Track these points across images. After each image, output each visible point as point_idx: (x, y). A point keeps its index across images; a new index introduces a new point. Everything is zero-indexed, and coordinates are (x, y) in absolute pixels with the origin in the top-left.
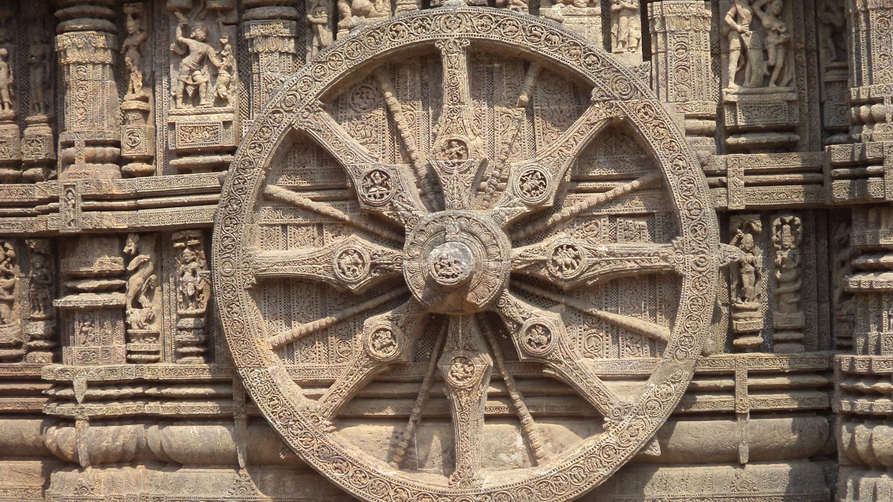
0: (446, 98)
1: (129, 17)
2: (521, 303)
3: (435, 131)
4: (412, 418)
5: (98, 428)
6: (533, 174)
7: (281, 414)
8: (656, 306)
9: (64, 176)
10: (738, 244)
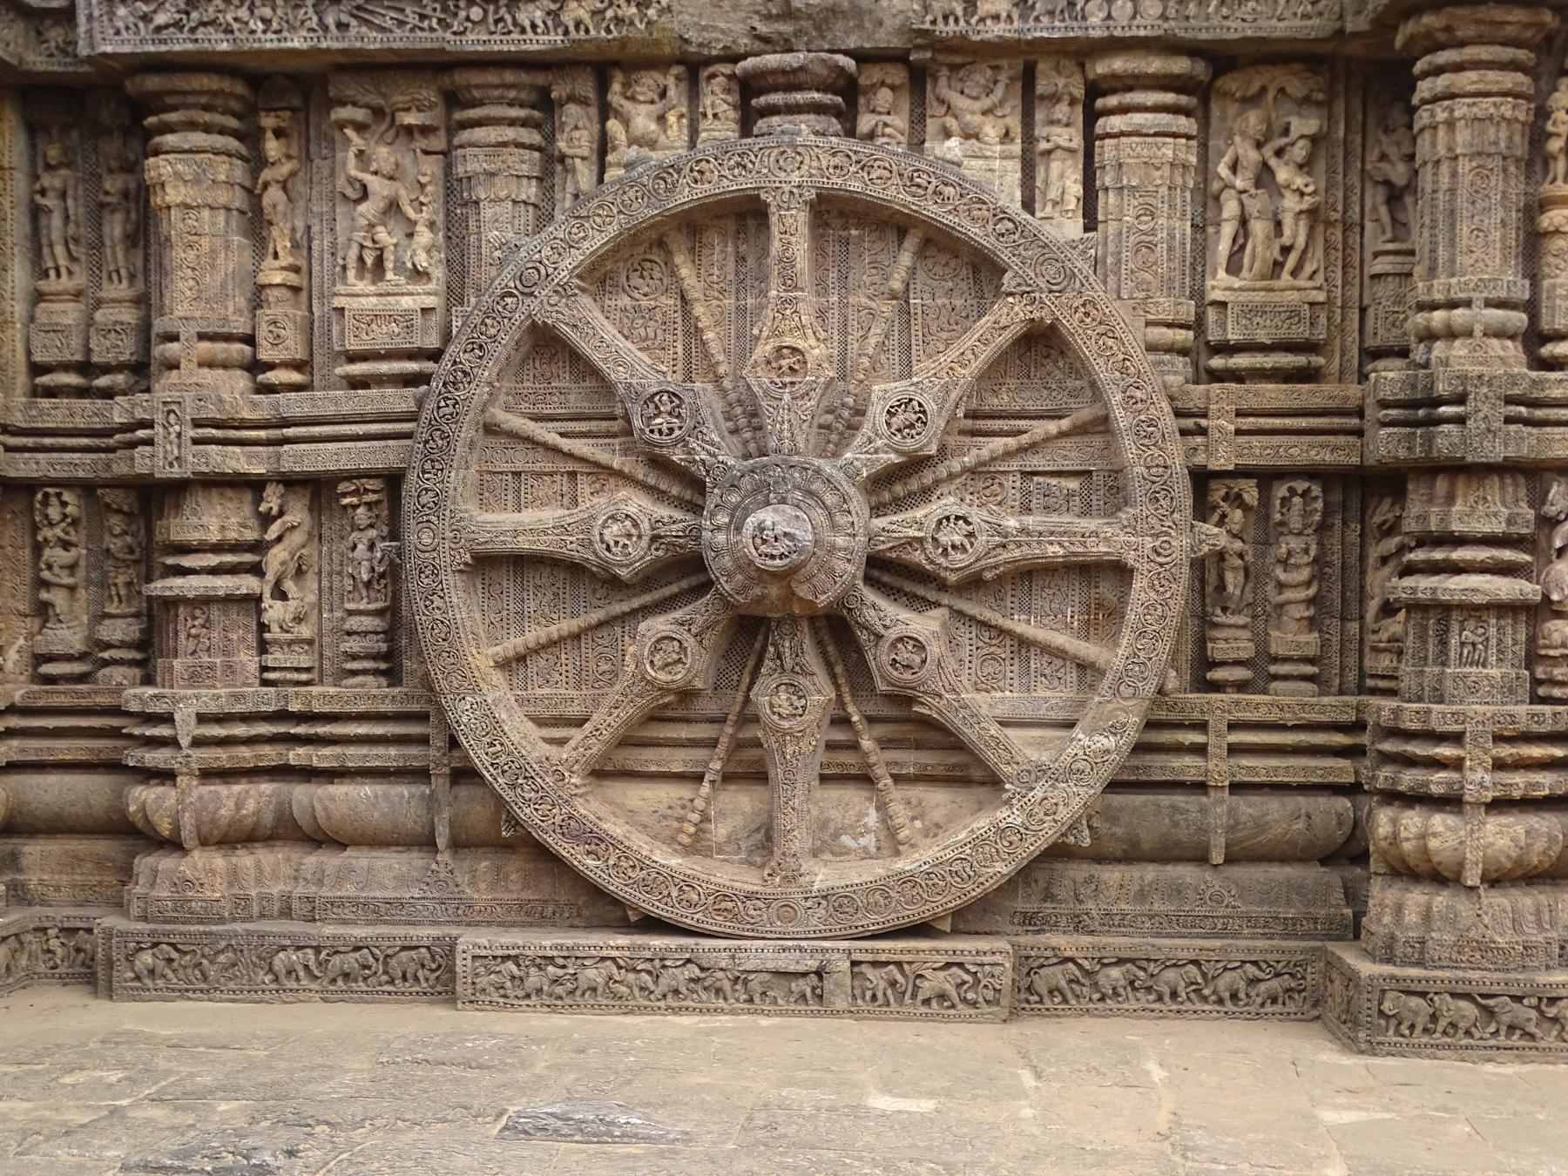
0: (775, 281)
1: (269, 134)
2: (882, 603)
3: (756, 332)
5: (213, 788)
8: (1088, 614)
9: (165, 387)
10: (1221, 523)
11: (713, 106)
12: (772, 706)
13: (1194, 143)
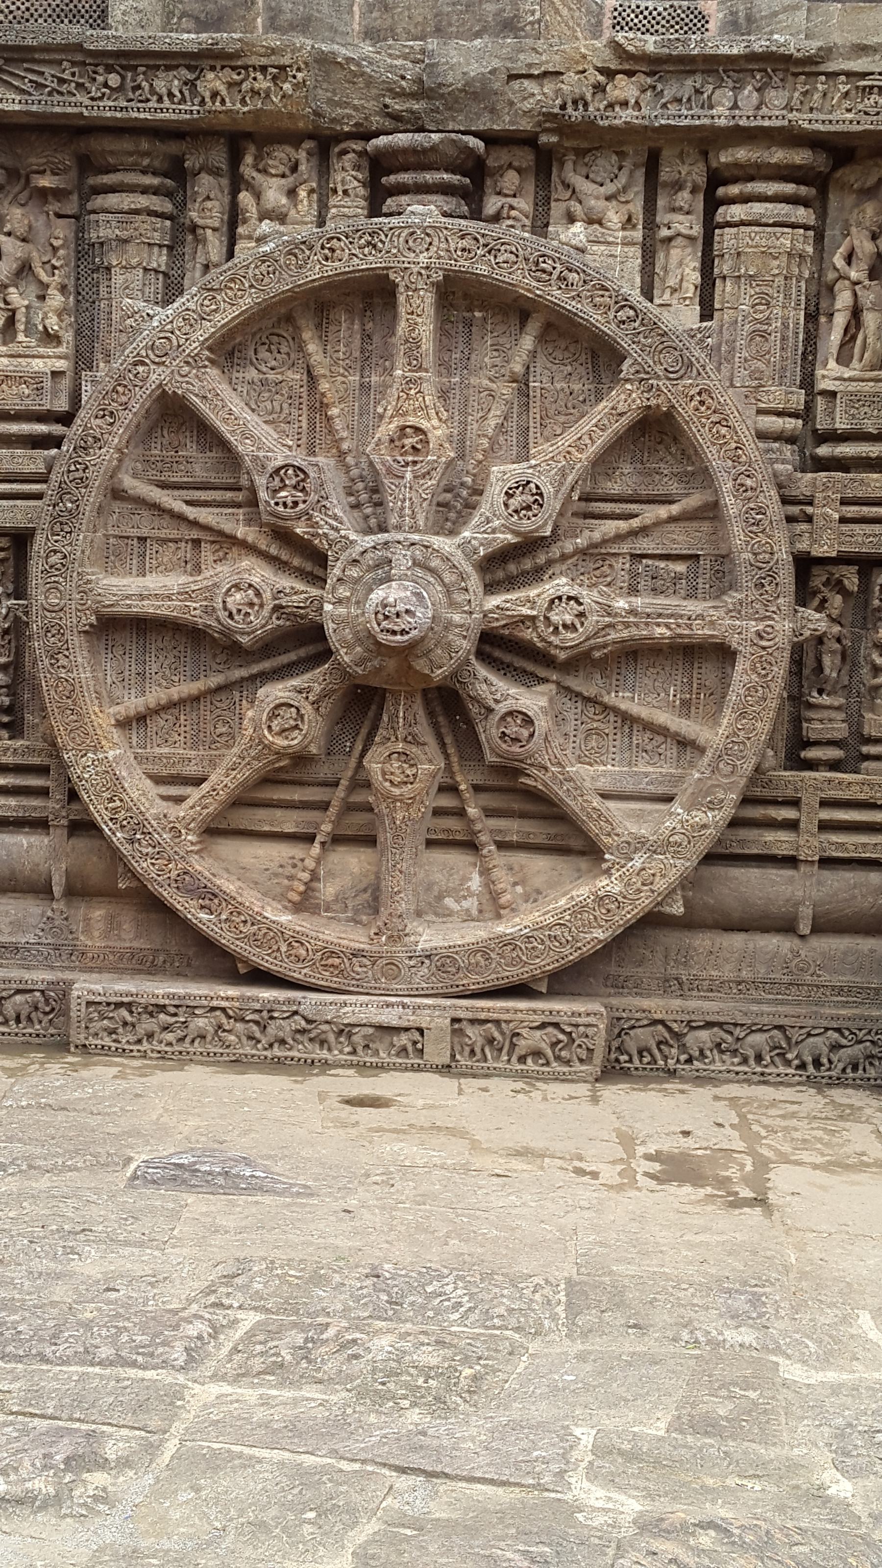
0: (401, 360)
2: (493, 678)
3: (380, 410)
4: (319, 839)
6: (524, 486)
7: (125, 823)
8: (691, 693)
11: (343, 182)
12: (384, 773)
13: (811, 233)
